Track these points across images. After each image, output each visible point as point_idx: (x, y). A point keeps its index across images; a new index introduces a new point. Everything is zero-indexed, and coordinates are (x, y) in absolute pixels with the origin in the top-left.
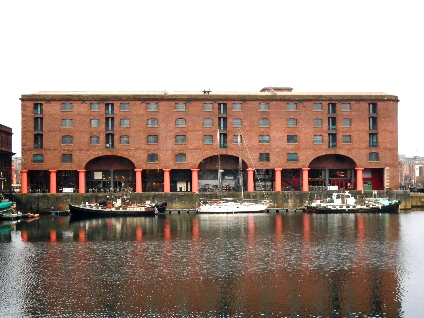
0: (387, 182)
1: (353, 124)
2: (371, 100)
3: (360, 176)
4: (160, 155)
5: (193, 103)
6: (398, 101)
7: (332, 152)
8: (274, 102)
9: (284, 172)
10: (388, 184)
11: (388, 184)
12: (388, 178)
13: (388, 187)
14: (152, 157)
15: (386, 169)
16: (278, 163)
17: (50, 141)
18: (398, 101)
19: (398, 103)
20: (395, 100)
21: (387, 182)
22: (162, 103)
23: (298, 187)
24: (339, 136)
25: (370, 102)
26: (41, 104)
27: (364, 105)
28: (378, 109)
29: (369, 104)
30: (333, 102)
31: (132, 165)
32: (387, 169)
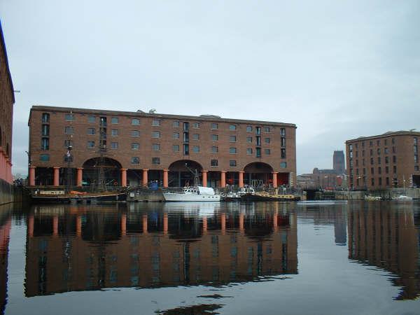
1: (271, 142)
3: (275, 177)
4: (141, 158)
5: (166, 121)
7: (258, 160)
8: (221, 124)
9: (227, 174)
14: (137, 161)
15: (291, 173)
16: (223, 168)
17: (56, 144)
20: (294, 127)
22: (143, 120)
24: (263, 150)
26: (48, 115)
27: (278, 129)
28: (286, 132)
30: (259, 125)
31: (119, 165)
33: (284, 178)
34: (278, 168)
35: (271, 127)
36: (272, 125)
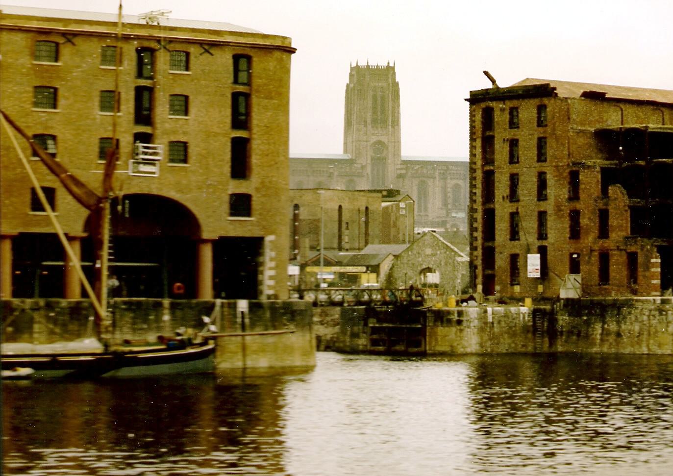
0: (271, 278)
2: (238, 45)
3: (207, 254)
6: (292, 51)
10: (272, 283)
11: (272, 283)
12: (273, 264)
13: (271, 292)
18: (292, 51)
19: (293, 55)
21: (271, 278)
23: (56, 284)
25: (239, 51)
27: (225, 59)
29: (236, 58)
32: (271, 242)
33: (239, 263)
34: (216, 223)
35: (193, 50)
36: (201, 43)
